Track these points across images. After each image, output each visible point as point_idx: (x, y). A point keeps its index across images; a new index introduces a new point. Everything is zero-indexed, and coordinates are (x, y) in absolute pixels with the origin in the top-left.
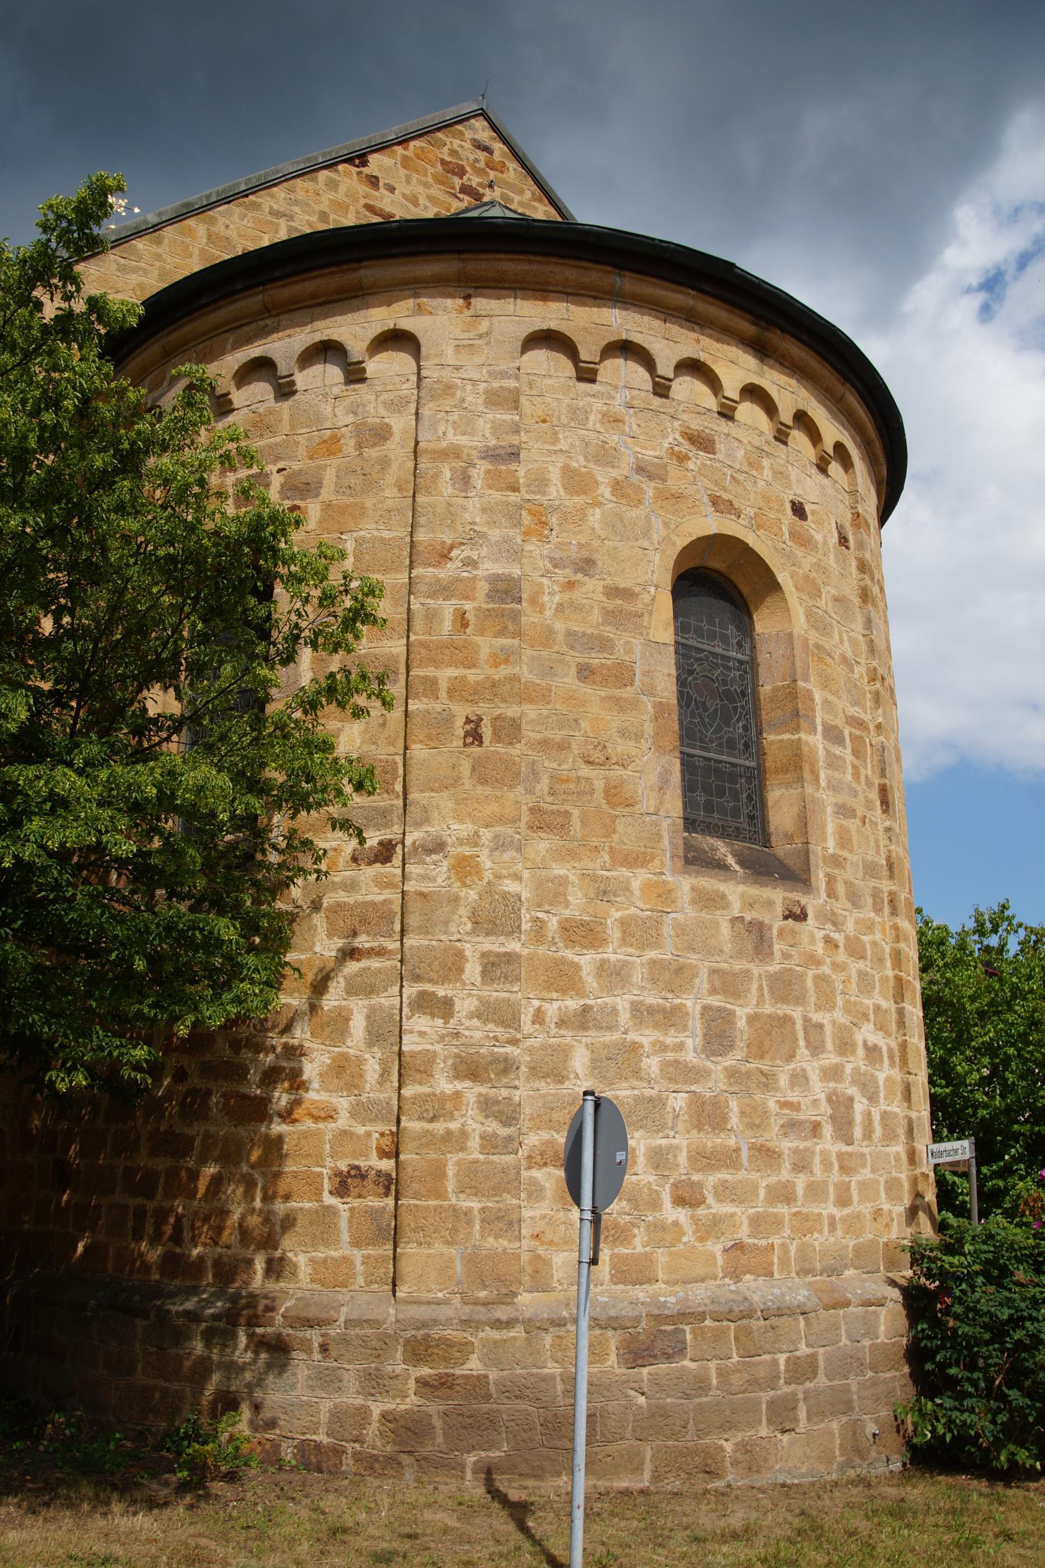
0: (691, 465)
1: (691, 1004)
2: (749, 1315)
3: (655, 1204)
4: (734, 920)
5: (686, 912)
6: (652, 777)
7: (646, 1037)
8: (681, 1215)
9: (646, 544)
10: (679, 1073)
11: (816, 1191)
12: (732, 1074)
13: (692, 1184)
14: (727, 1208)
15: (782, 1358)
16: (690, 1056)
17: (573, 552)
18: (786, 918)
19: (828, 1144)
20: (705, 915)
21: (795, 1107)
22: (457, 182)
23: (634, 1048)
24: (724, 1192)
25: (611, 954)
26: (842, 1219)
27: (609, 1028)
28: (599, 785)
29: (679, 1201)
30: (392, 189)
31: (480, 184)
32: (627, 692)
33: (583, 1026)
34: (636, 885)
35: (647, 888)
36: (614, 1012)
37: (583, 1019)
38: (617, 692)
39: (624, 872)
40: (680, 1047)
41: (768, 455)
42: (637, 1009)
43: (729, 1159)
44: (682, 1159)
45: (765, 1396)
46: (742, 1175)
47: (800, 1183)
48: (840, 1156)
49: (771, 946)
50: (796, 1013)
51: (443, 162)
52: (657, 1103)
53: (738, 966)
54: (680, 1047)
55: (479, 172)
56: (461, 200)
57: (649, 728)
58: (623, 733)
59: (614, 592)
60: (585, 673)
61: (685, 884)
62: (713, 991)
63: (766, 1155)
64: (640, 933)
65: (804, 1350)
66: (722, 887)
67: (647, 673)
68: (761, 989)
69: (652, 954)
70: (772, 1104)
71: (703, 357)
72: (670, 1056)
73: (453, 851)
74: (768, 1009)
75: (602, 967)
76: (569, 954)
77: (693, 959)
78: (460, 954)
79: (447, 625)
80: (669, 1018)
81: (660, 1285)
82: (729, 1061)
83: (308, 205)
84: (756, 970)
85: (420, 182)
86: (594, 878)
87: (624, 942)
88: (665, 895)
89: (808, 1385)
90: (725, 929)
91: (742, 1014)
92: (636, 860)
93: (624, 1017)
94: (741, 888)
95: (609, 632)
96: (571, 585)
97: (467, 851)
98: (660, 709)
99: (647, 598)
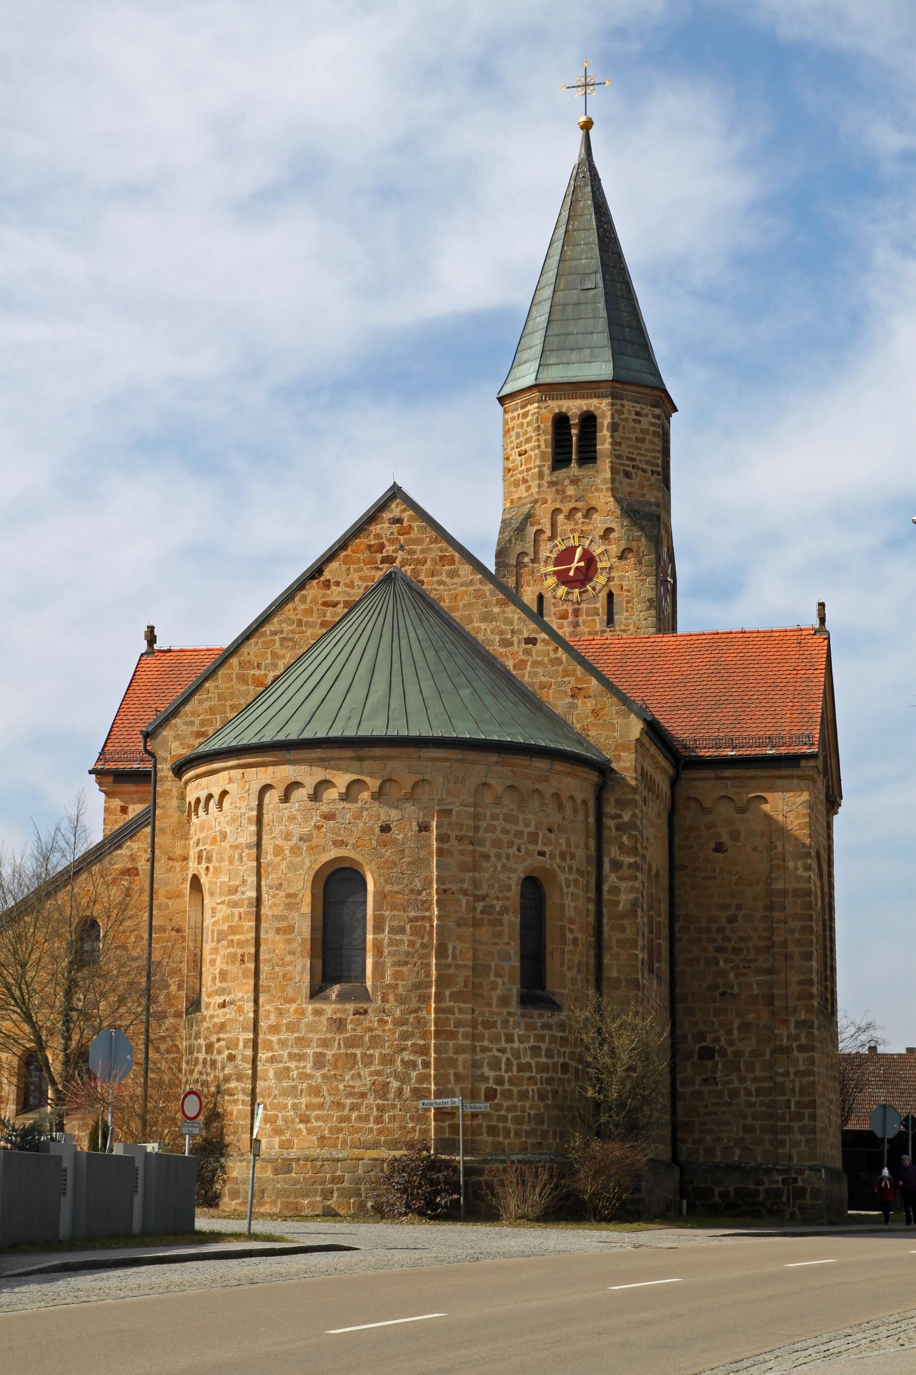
0: (324, 830)
1: (310, 1051)
2: (317, 1160)
3: (293, 1122)
4: (328, 1019)
5: (309, 1018)
6: (299, 968)
7: (292, 1065)
8: (302, 1126)
9: (301, 872)
10: (304, 1076)
11: (359, 1118)
12: (324, 1076)
13: (305, 1115)
14: (319, 1124)
15: (328, 1176)
16: (309, 1071)
17: (276, 882)
18: (354, 1015)
19: (371, 1100)
20: (317, 1018)
21: (353, 1087)
22: (379, 556)
23: (288, 1069)
24: (318, 1118)
25: (283, 1037)
26: (377, 1129)
27: (281, 1062)
28: (281, 974)
29: (301, 1121)
30: (337, 584)
31: (394, 551)
32: (291, 937)
33: (272, 1062)
34: (291, 1010)
35: (296, 1010)
36: (283, 1056)
37: (272, 1060)
38: (288, 937)
39: (287, 1006)
40: (304, 1067)
41: (367, 809)
42: (290, 1054)
43: (321, 1106)
44: (303, 1106)
45: (320, 1187)
46: (325, 1112)
47: (354, 1115)
48: (378, 1105)
49: (345, 1026)
50: (358, 1052)
51: (370, 547)
52: (295, 1087)
53: (329, 1036)
54: (304, 1067)
55: (392, 541)
56: (381, 569)
57: (299, 950)
58: (289, 953)
59: (290, 896)
60: (278, 931)
61: (309, 1008)
62: (318, 1046)
63: (339, 1105)
64: (292, 1027)
65: (339, 1173)
66: (324, 1007)
67: (299, 927)
68: (339, 1044)
69: (296, 1035)
70: (341, 1087)
71: (328, 777)
72: (301, 1070)
73: (237, 1004)
74: (343, 1051)
75: (279, 1041)
76: (269, 1037)
77: (310, 1035)
78: (238, 1039)
79: (236, 918)
80: (301, 1057)
81: (294, 1150)
82: (325, 1071)
83: (289, 619)
84: (337, 1037)
85: (356, 570)
86: (278, 1009)
87: (286, 1031)
88: (303, 1013)
89: (339, 1185)
90: (325, 1023)
91: (329, 1053)
92: (292, 1000)
93: (286, 1058)
94: (333, 1006)
95: (286, 913)
96: (274, 896)
97: (240, 1003)
98: (303, 941)
99: (300, 895)
